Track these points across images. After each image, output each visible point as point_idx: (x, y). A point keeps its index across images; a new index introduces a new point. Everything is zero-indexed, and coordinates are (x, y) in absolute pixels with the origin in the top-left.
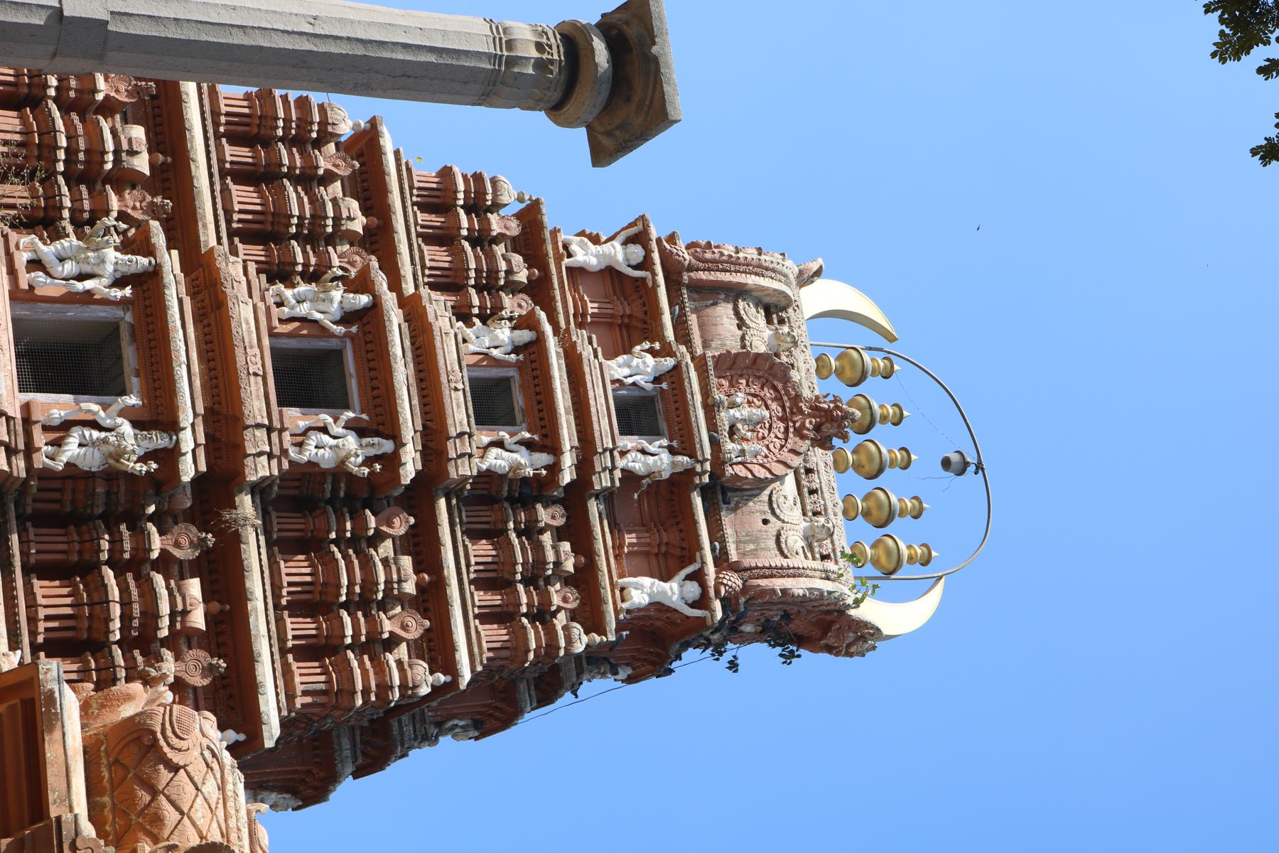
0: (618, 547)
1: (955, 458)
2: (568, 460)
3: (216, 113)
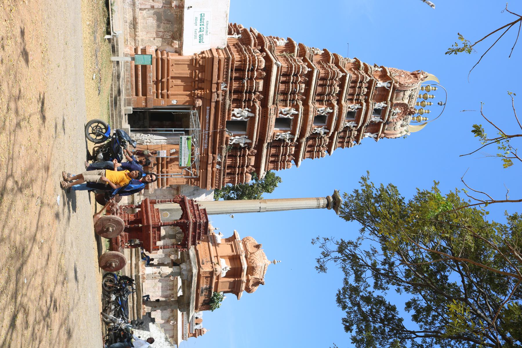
1: (440, 103)
3: (318, 77)
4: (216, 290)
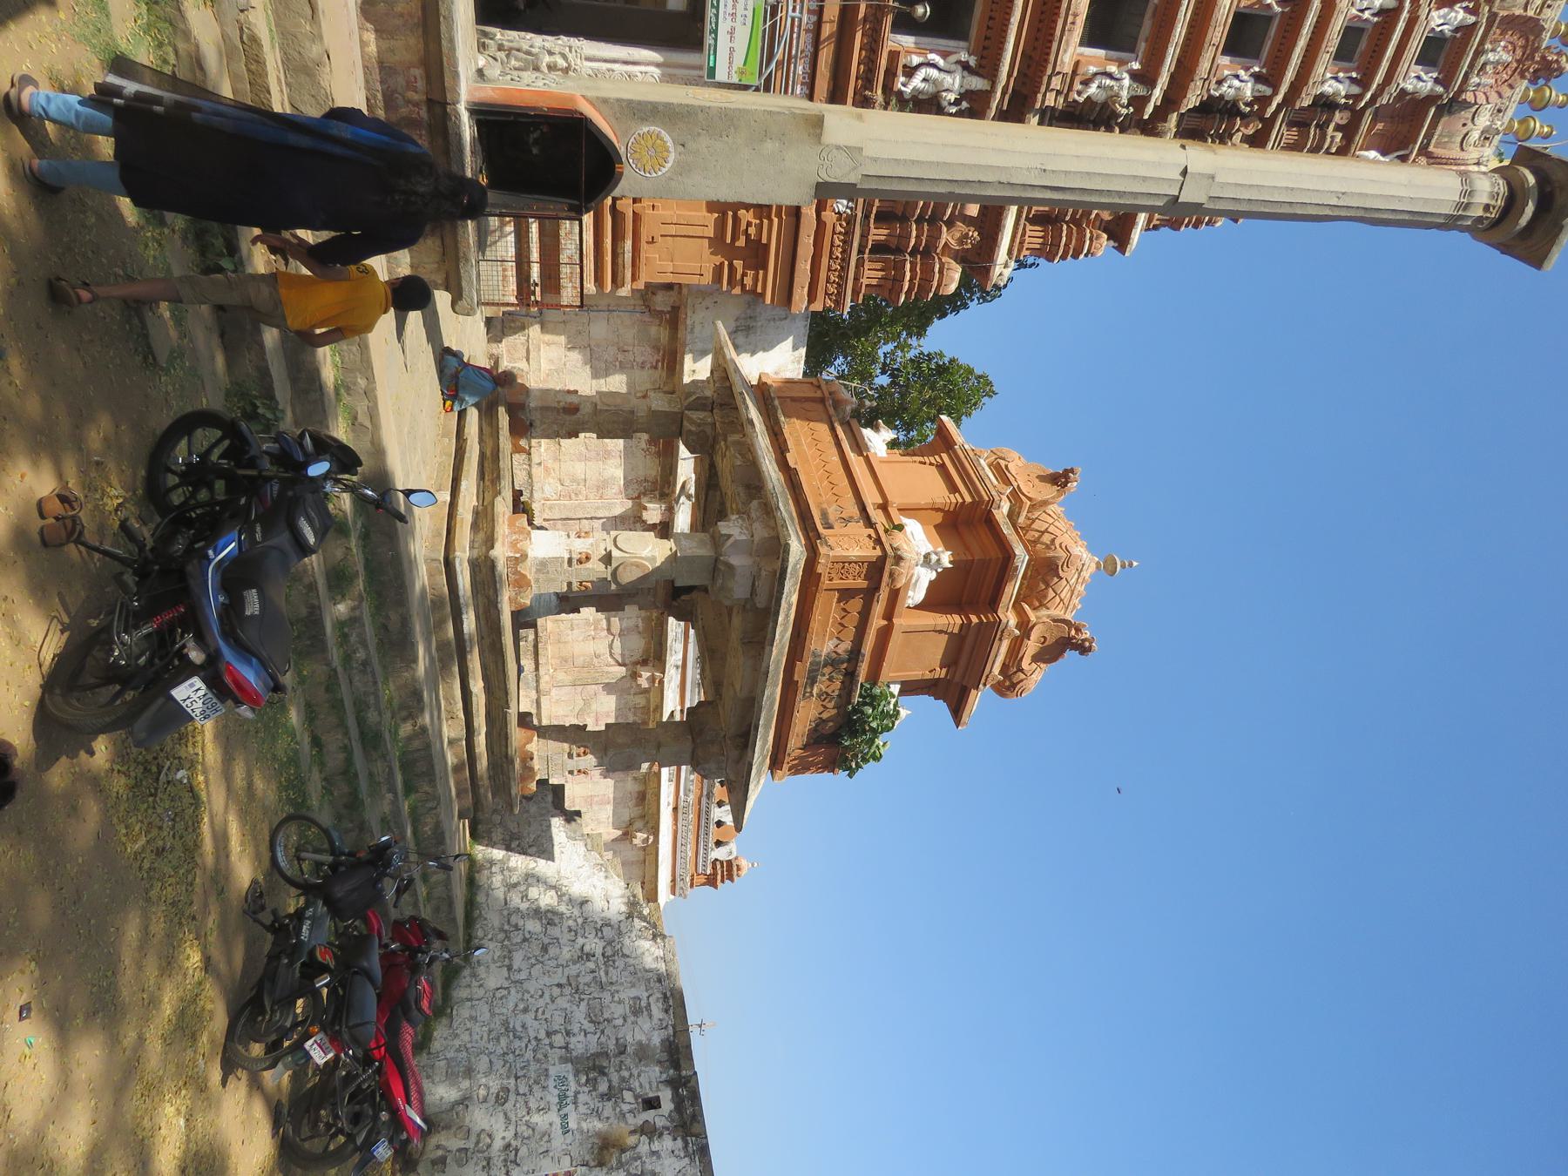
0: (1370, 130)
2: (1368, 96)
4: (874, 677)
